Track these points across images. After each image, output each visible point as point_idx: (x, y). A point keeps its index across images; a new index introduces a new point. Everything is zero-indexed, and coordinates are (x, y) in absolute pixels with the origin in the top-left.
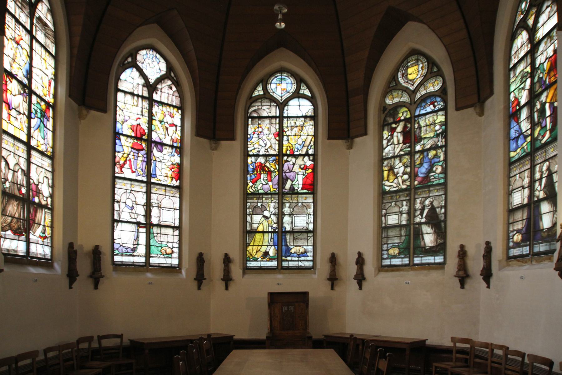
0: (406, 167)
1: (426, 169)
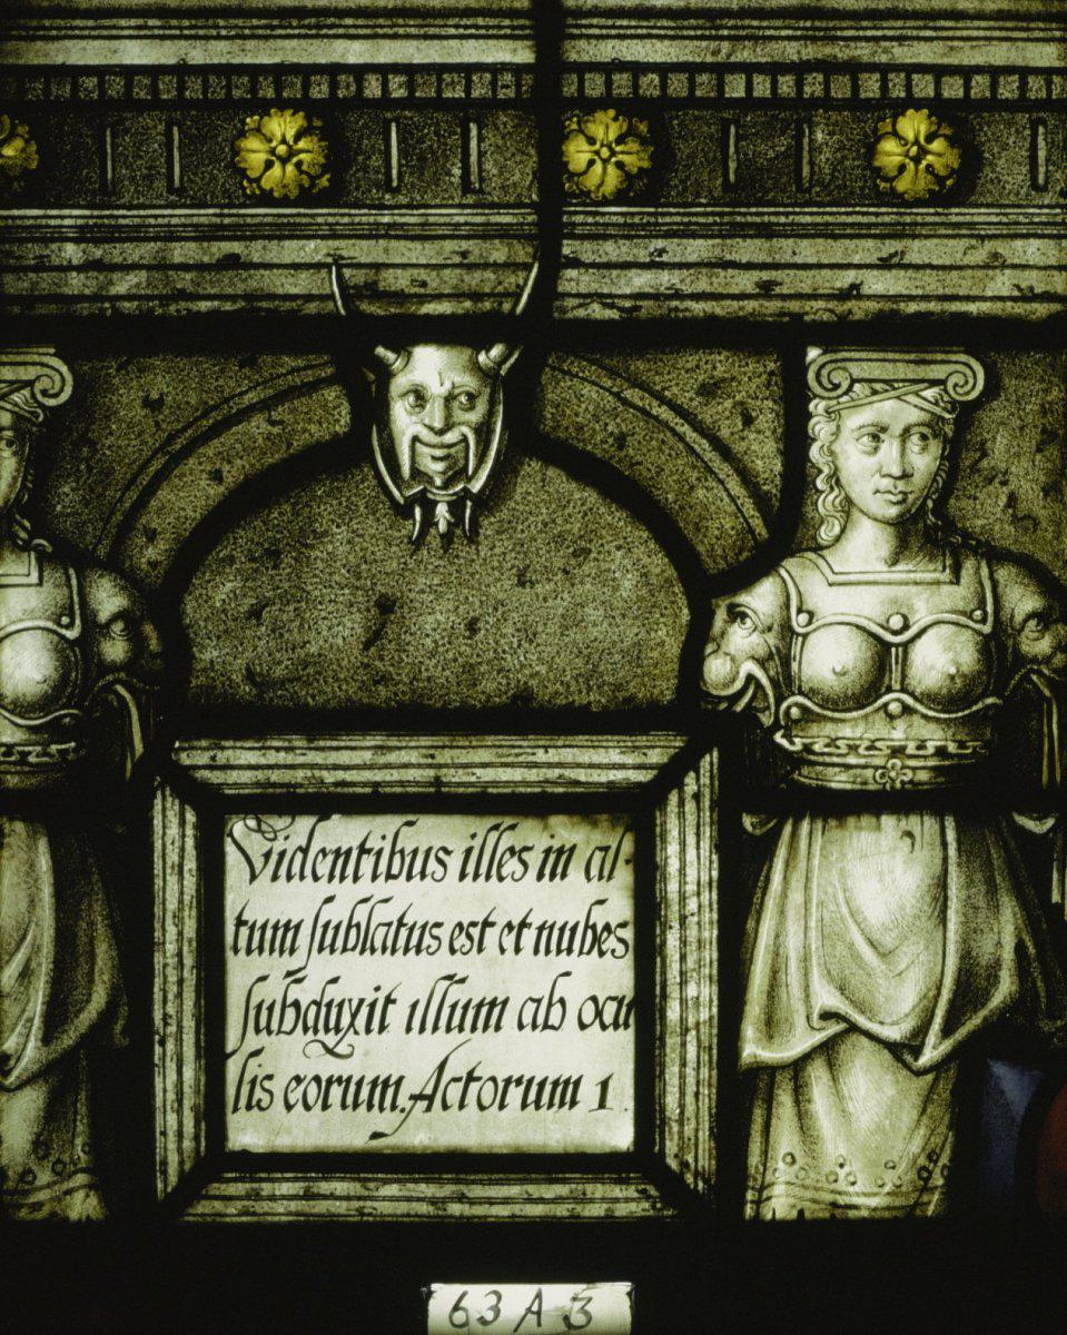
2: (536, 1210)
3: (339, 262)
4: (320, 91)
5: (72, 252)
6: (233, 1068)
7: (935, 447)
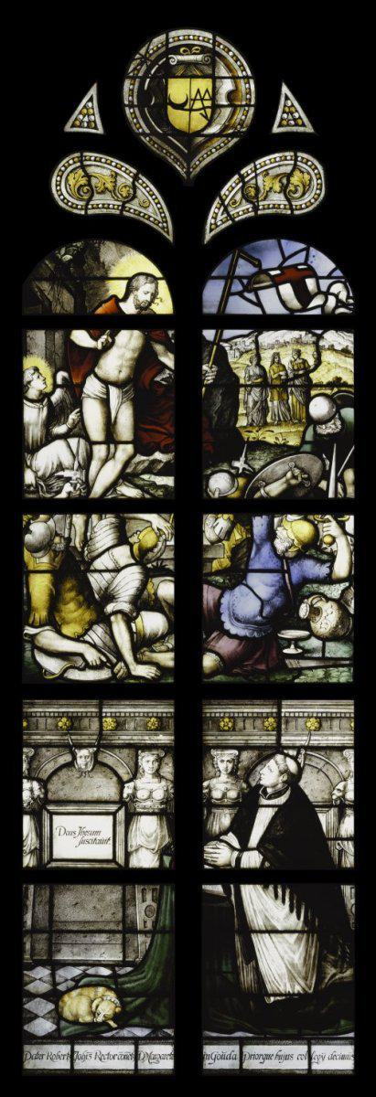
0: (151, 572)
1: (263, 603)
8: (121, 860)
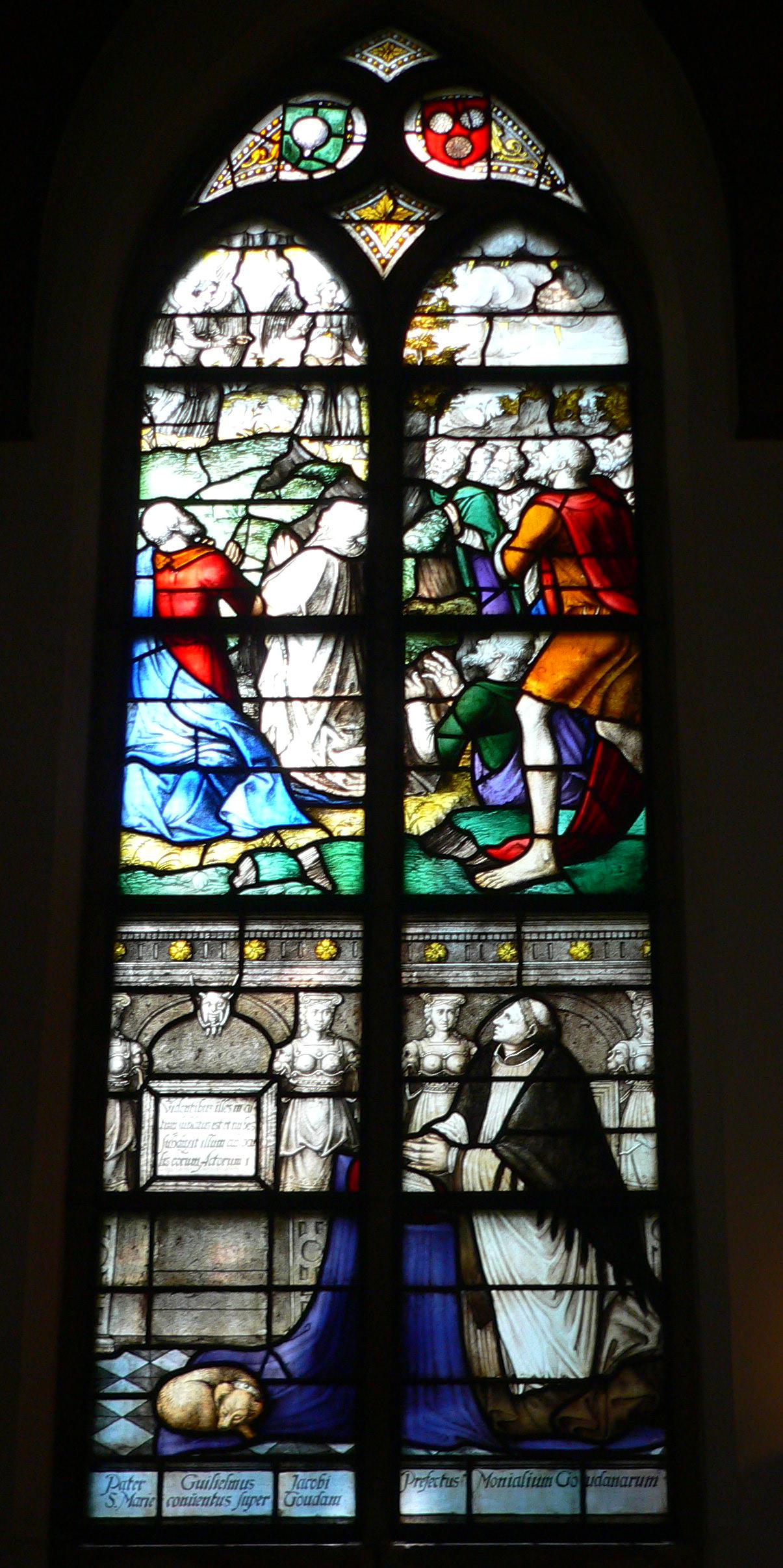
2: (230, 1189)
3: (192, 974)
4: (189, 937)
5: (131, 972)
6: (159, 1156)
7: (330, 1015)
8: (268, 1175)
